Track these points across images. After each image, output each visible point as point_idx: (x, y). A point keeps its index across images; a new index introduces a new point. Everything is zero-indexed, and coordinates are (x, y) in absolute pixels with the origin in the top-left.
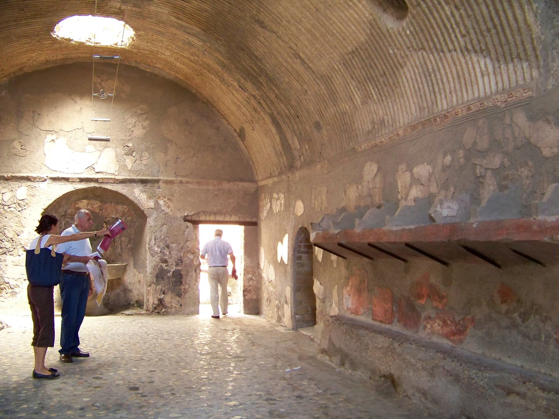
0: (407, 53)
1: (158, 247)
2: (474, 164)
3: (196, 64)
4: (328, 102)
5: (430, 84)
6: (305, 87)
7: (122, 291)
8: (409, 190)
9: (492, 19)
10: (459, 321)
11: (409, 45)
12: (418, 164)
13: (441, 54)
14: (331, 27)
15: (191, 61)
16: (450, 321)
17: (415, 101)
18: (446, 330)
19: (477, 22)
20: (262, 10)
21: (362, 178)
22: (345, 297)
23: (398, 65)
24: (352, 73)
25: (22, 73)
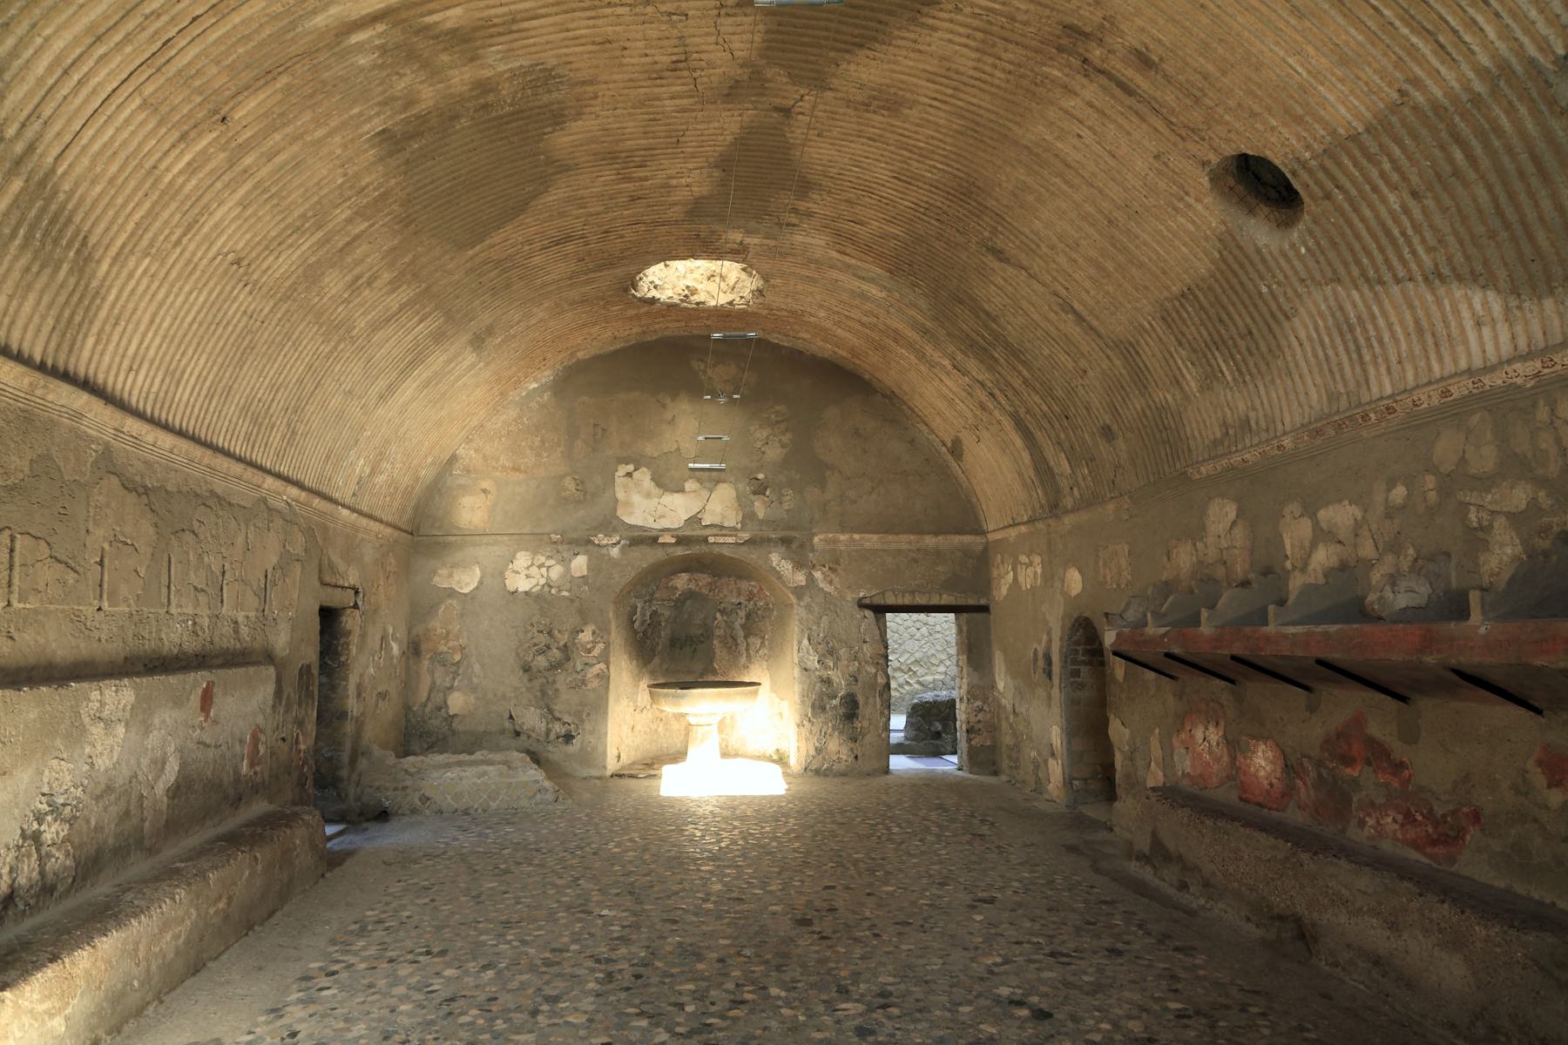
0: (1300, 289)
2: (1461, 503)
3: (872, 331)
4: (1128, 390)
5: (1352, 347)
6: (1083, 363)
8: (1311, 552)
9: (1500, 213)
10: (1444, 816)
11: (1304, 275)
12: (1327, 504)
13: (1378, 288)
14: (1137, 252)
15: (863, 325)
16: (1422, 814)
17: (1319, 380)
18: (1412, 833)
19: (1464, 219)
20: (1000, 228)
21: (1203, 528)
22: (1176, 752)
23: (1279, 314)
24: (1180, 336)
25: (574, 360)
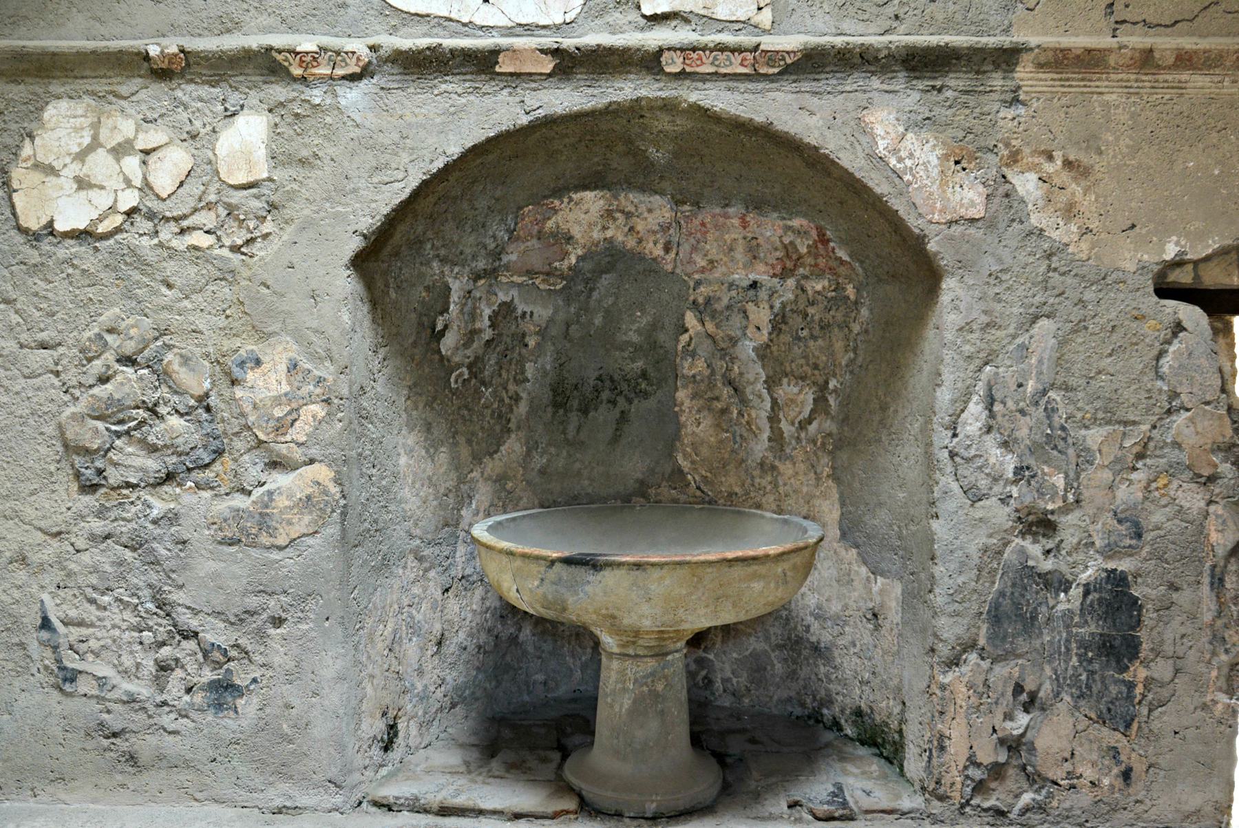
1: (1005, 444)
7: (780, 647)
